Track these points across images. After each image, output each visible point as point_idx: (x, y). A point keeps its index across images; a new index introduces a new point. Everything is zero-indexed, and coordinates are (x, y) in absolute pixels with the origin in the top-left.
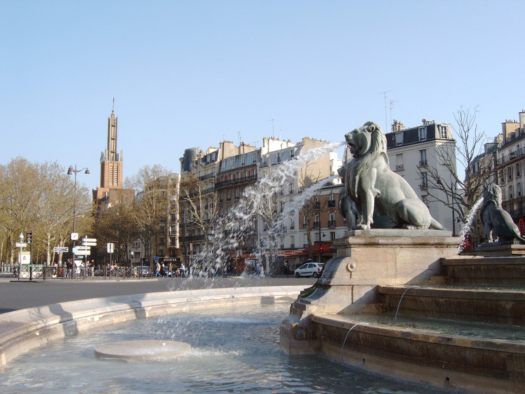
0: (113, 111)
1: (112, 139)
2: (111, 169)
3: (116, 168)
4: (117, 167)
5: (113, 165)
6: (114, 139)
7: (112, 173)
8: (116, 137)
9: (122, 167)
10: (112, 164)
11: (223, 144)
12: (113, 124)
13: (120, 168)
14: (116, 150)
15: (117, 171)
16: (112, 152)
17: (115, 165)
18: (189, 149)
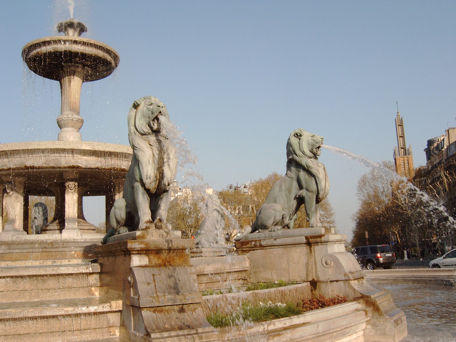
0: (398, 113)
1: (400, 137)
2: (402, 163)
3: (407, 161)
4: (408, 161)
5: (404, 159)
6: (402, 137)
7: (404, 167)
8: (403, 134)
9: (412, 160)
10: (403, 159)
11: (448, 131)
12: (400, 124)
13: (410, 161)
14: (405, 146)
15: (408, 164)
16: (402, 148)
17: (406, 159)
18: (431, 139)
